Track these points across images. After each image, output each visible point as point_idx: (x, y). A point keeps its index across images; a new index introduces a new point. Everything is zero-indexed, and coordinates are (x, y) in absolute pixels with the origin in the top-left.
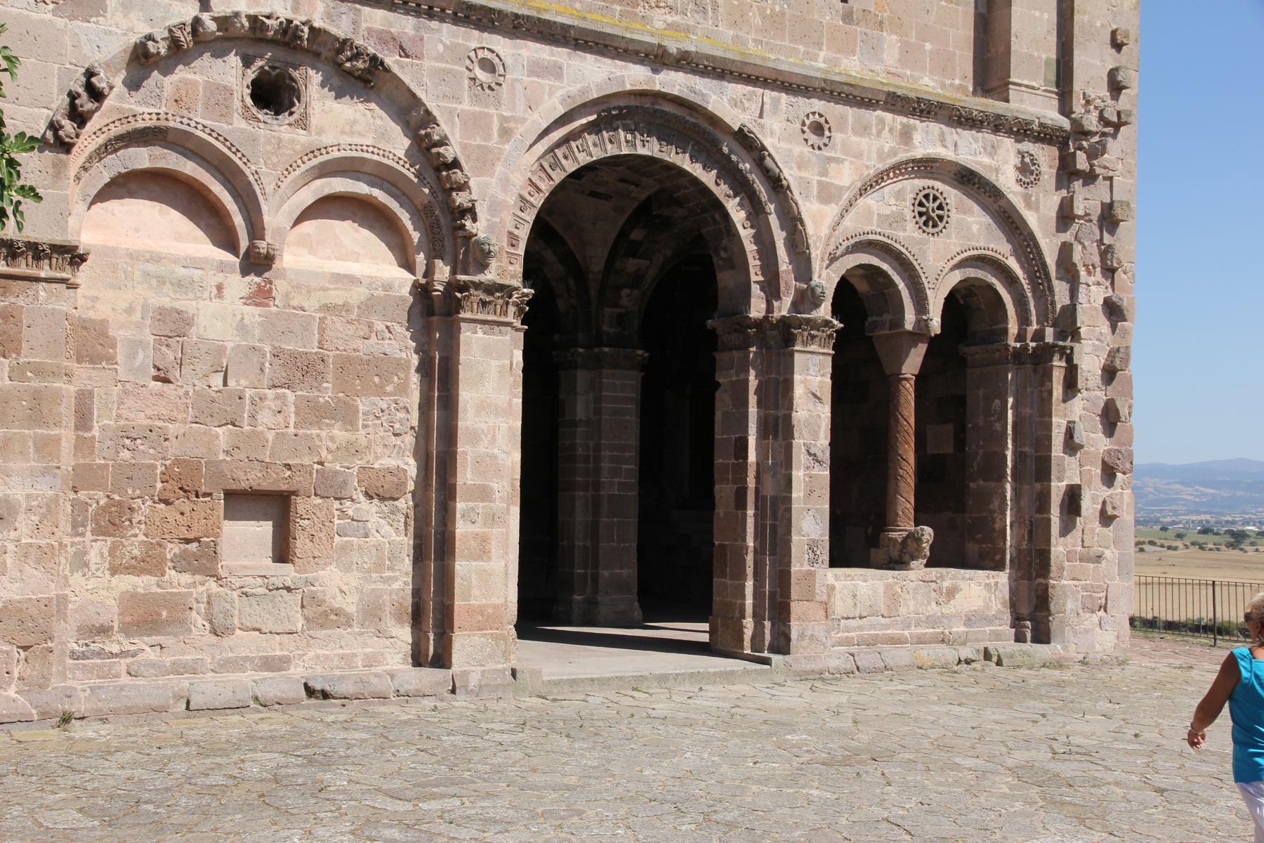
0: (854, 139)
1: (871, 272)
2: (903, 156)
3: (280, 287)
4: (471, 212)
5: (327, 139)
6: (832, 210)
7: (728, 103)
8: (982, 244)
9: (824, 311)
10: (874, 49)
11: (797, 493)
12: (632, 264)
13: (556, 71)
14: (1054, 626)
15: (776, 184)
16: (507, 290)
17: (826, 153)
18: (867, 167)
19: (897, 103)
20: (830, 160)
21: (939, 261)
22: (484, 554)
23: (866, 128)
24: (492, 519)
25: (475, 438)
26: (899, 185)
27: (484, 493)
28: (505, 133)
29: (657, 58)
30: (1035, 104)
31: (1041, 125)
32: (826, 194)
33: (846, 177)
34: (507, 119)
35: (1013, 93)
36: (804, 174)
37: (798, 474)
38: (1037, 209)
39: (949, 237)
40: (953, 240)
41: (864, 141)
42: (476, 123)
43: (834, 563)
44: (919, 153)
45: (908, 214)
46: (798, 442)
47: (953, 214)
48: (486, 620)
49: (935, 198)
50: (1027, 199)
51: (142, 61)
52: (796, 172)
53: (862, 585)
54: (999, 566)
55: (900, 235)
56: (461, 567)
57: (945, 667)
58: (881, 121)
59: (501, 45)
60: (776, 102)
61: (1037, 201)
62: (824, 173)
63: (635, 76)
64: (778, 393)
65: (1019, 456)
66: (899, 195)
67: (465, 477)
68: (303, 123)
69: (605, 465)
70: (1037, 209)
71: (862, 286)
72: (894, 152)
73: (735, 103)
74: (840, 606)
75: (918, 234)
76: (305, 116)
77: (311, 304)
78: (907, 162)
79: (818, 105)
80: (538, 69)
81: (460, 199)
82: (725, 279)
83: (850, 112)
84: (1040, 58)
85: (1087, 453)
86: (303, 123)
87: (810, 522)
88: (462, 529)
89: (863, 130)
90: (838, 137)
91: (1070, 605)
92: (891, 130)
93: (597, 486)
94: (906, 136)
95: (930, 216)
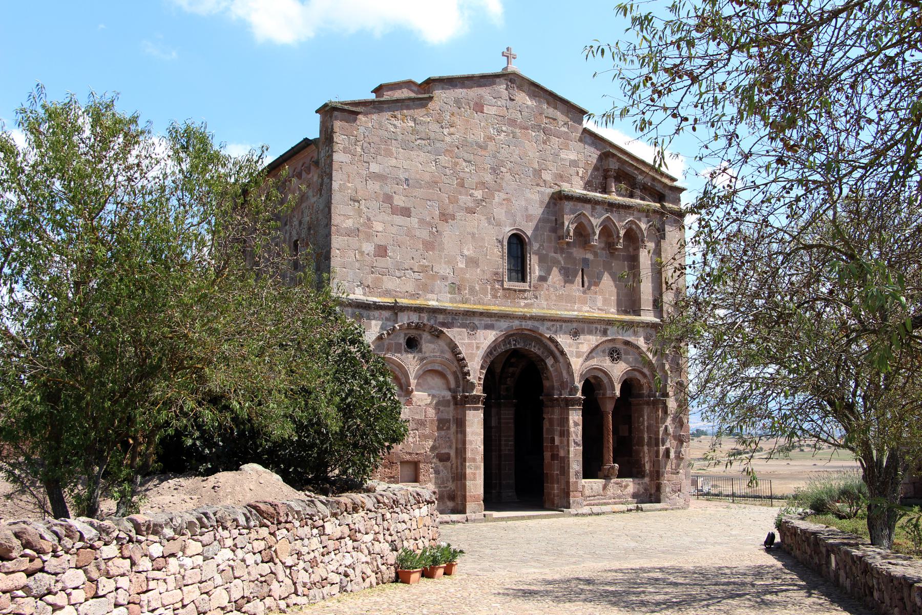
1: (596, 378)
3: (414, 399)
4: (468, 373)
5: (427, 355)
6: (581, 360)
9: (579, 395)
11: (571, 455)
12: (511, 370)
14: (662, 496)
15: (562, 353)
16: (479, 397)
21: (618, 371)
22: (474, 479)
24: (477, 468)
25: (471, 442)
27: (474, 460)
28: (478, 348)
29: (523, 318)
30: (648, 317)
32: (578, 355)
33: (585, 348)
35: (642, 312)
37: (572, 449)
42: (470, 345)
43: (584, 478)
46: (571, 438)
47: (623, 356)
48: (475, 499)
53: (596, 484)
54: (643, 477)
56: (468, 483)
57: (623, 512)
58: (596, 328)
60: (561, 326)
64: (564, 421)
65: (650, 438)
67: (469, 455)
68: (420, 351)
69: (503, 443)
71: (593, 381)
73: (548, 329)
74: (587, 492)
75: (610, 364)
76: (421, 349)
77: (422, 404)
79: (575, 325)
81: (466, 369)
82: (546, 384)
83: (586, 326)
86: (420, 351)
87: (576, 466)
88: (468, 471)
91: (667, 490)
93: (500, 450)
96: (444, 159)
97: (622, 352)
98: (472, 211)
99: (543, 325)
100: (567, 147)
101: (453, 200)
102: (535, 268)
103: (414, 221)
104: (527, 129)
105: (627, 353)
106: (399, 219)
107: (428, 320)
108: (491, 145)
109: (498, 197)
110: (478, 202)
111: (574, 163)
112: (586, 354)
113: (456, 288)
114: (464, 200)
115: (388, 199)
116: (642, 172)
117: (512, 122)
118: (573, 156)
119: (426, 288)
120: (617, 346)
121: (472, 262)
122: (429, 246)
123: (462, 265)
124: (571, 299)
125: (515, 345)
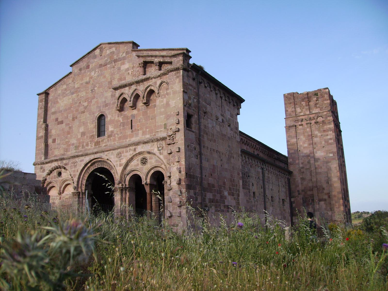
0: (126, 154)
2: (134, 154)
6: (122, 168)
7: (104, 156)
8: (155, 164)
10: (137, 135)
13: (82, 161)
17: (120, 158)
18: (128, 158)
19: (130, 145)
20: (121, 159)
23: (127, 151)
26: (138, 158)
31: (160, 138)
32: (121, 165)
33: (124, 161)
34: (77, 169)
36: (117, 163)
38: (163, 154)
39: (148, 165)
40: (149, 165)
41: (127, 154)
42: (74, 171)
44: (137, 152)
45: (139, 163)
49: (145, 158)
50: (160, 153)
51: (49, 174)
52: (116, 163)
55: (138, 167)
58: (130, 149)
59: (77, 159)
60: (112, 153)
61: (163, 153)
62: (120, 161)
63: (92, 157)
66: (138, 160)
70: (163, 154)
72: (133, 154)
73: (106, 155)
75: (142, 166)
78: (136, 154)
79: (119, 150)
80: (82, 161)
83: (124, 150)
84: (163, 124)
85: (173, 203)
89: (127, 152)
90: (123, 155)
92: (132, 150)
94: (135, 150)
95: (144, 161)
96: (74, 95)
97: (148, 158)
98: (83, 112)
99: (104, 154)
100: (123, 64)
101: (77, 110)
102: (110, 128)
103: (64, 125)
104: (106, 65)
105: (150, 158)
106: (60, 126)
107: (61, 164)
108: (91, 80)
109: (94, 101)
110: (86, 108)
111: (128, 70)
112: (124, 164)
113: (77, 147)
114: (81, 109)
115: (57, 119)
116: (156, 56)
117: (101, 66)
118: (126, 66)
119: (66, 150)
120: (145, 156)
121: (83, 134)
122: (69, 133)
123: (79, 136)
124: (125, 137)
125: (97, 166)
